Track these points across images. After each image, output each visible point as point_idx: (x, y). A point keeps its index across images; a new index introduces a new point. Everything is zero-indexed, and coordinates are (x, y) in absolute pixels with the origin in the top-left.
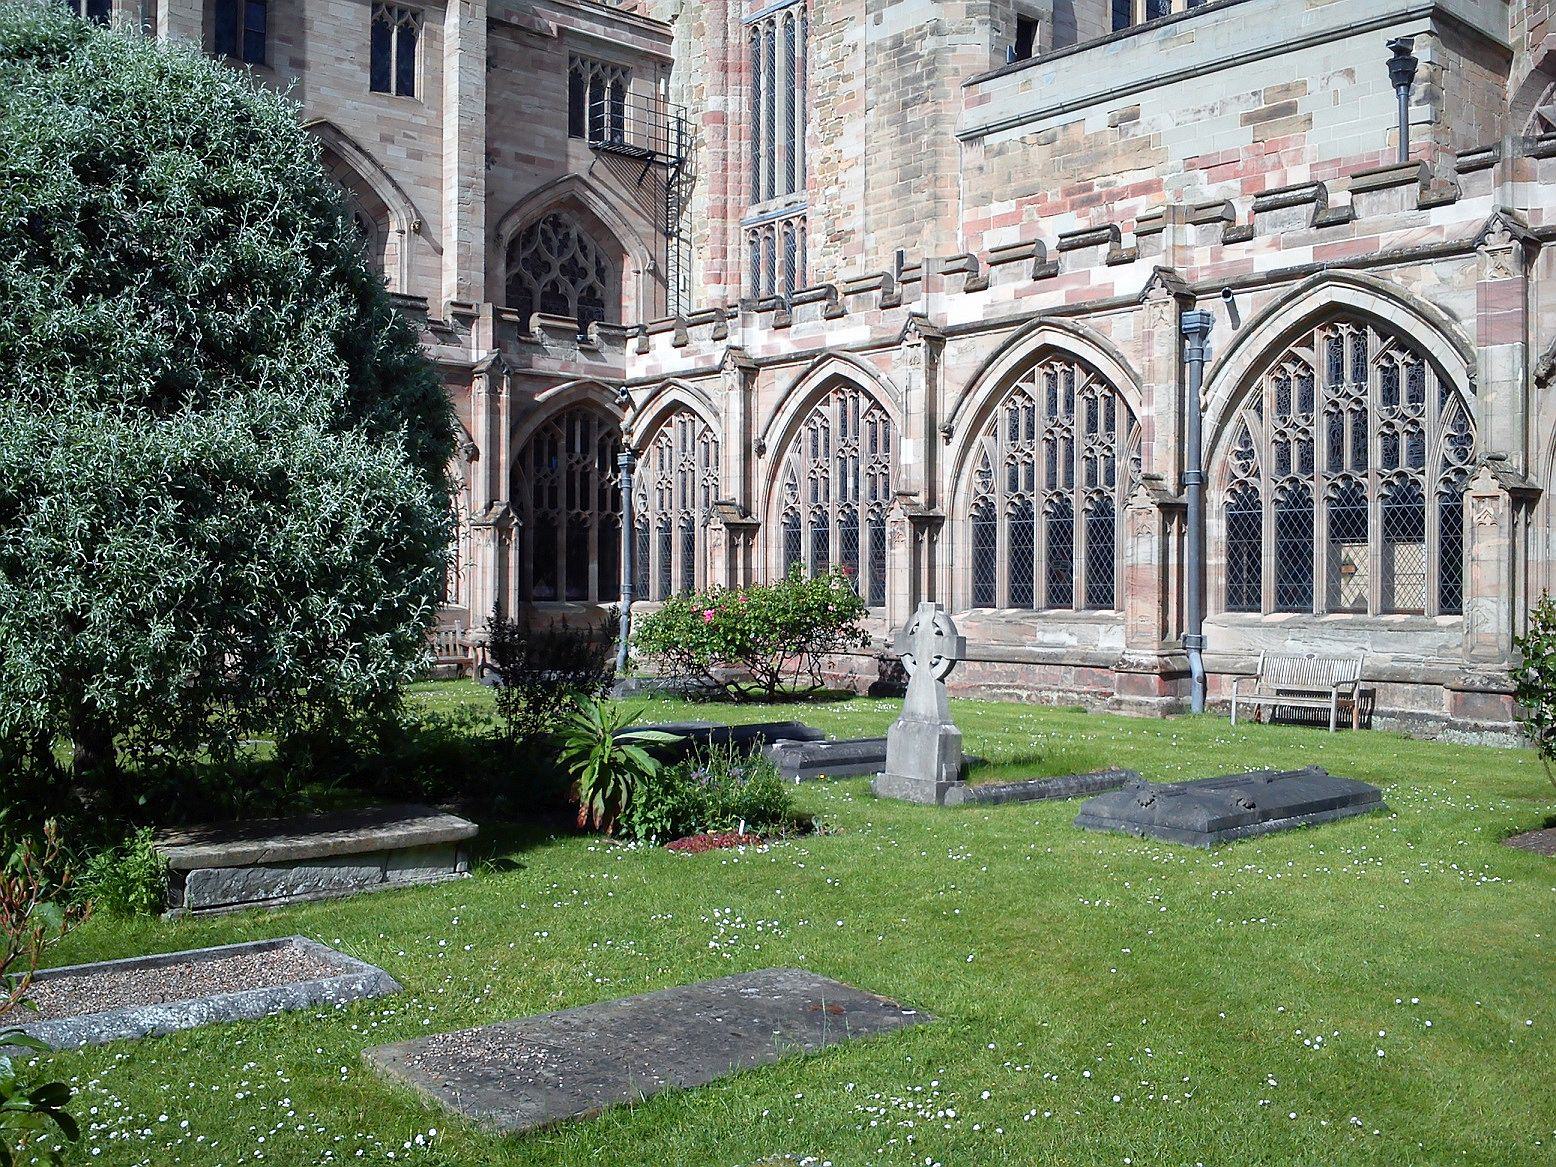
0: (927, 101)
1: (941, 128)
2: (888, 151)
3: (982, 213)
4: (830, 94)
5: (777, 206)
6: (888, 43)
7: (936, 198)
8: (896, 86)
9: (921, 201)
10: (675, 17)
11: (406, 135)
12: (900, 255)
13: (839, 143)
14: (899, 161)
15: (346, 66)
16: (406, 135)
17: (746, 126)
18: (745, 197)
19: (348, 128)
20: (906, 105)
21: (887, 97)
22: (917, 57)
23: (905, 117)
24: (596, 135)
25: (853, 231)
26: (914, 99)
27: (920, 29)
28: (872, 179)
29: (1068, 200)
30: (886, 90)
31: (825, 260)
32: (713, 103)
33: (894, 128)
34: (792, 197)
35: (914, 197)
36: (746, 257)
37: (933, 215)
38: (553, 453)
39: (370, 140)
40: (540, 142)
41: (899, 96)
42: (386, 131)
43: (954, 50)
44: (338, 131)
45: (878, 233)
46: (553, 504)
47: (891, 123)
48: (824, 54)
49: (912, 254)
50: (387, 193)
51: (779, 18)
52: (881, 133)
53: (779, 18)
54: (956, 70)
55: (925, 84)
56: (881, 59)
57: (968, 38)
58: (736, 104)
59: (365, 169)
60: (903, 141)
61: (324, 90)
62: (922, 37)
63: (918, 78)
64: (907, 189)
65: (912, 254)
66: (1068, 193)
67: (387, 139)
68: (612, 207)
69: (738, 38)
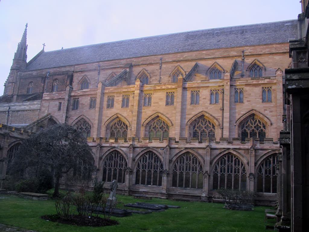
11: (269, 109)
16: (269, 109)
19: (258, 109)
38: (270, 164)
39: (262, 111)
42: (265, 109)
44: (255, 110)
46: (270, 174)
50: (266, 119)
67: (265, 110)
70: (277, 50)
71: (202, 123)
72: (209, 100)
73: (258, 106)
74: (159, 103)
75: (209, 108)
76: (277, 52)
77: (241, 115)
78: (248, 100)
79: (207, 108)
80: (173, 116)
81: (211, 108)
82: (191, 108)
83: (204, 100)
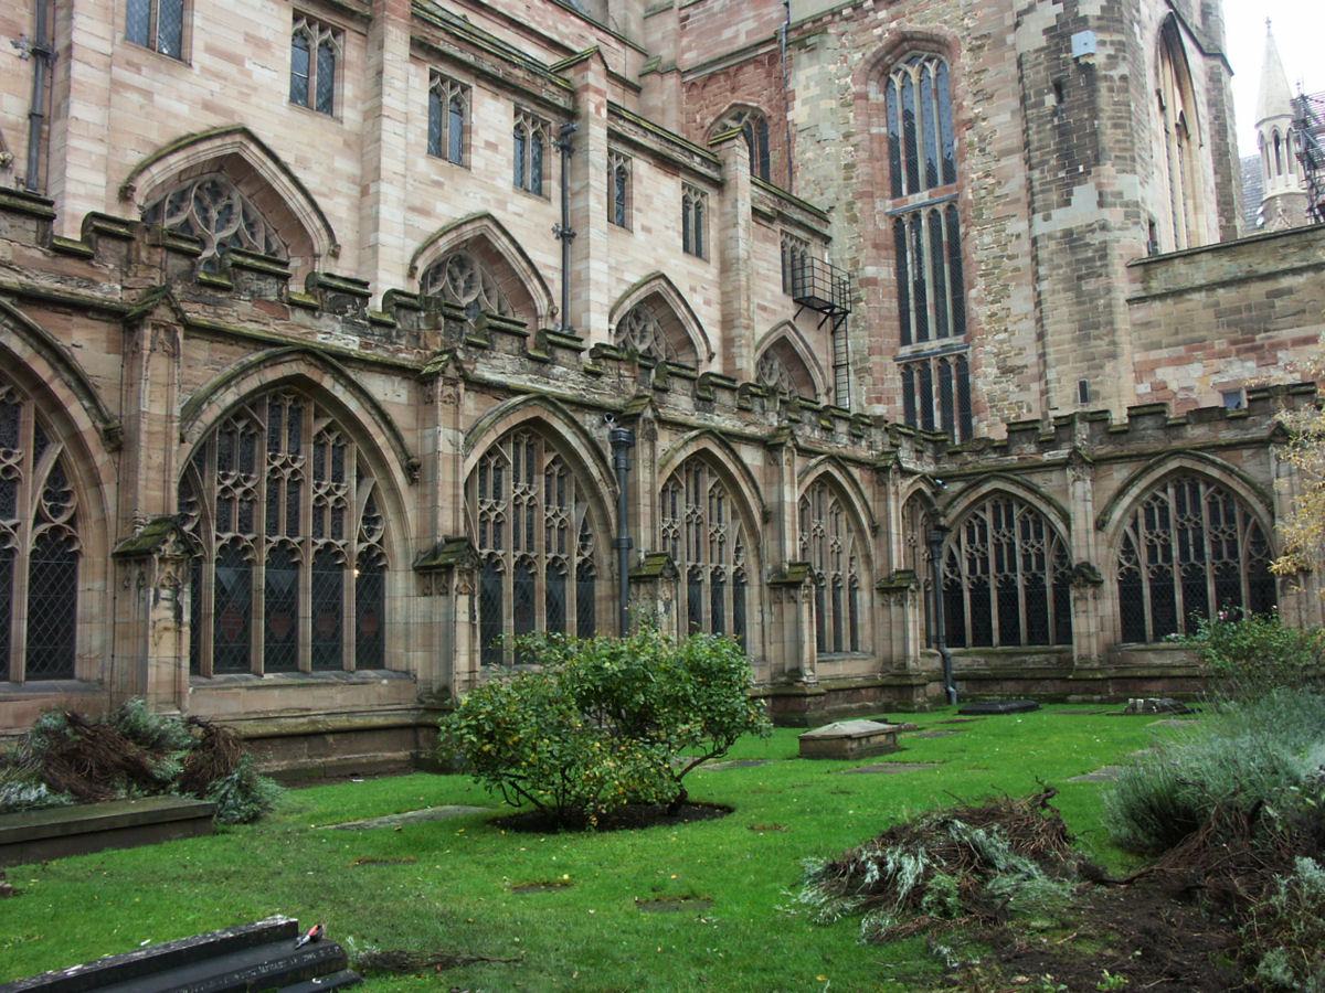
0: (1101, 275)
1: (1113, 295)
2: (1065, 309)
3: (1154, 355)
4: (995, 268)
5: (933, 344)
6: (1059, 234)
7: (1114, 343)
8: (1069, 264)
9: (1102, 345)
10: (832, 208)
12: (1083, 386)
13: (1006, 303)
14: (1077, 317)
15: (671, 233)
17: (894, 289)
18: (896, 340)
20: (1080, 278)
21: (1061, 272)
22: (1088, 245)
23: (1079, 287)
24: (794, 289)
25: (1026, 366)
26: (1088, 274)
27: (1091, 225)
28: (1050, 328)
29: (1233, 348)
30: (1059, 267)
31: (997, 387)
32: (870, 271)
33: (1070, 294)
34: (946, 341)
35: (1093, 343)
36: (899, 384)
37: (1113, 356)
40: (769, 295)
41: (1074, 270)
42: (693, 283)
43: (1118, 241)
44: (669, 283)
45: (1059, 368)
47: (1066, 290)
48: (987, 239)
49: (1096, 383)
50: (693, 331)
51: (924, 213)
52: (1056, 296)
53: (924, 213)
54: (1121, 256)
55: (1098, 264)
56: (1052, 245)
57: (1126, 233)
58: (884, 272)
59: (681, 312)
60: (1079, 303)
61: (660, 251)
62: (1093, 231)
63: (1092, 259)
64: (1088, 337)
65: (1096, 383)
66: (1234, 342)
67: (693, 289)
68: (807, 346)
69: (885, 226)
70: (533, 18)
71: (453, 280)
72: (508, 160)
73: (673, 261)
74: (248, 65)
75: (510, 207)
76: (533, 26)
77: (625, 287)
78: (646, 223)
79: (502, 204)
80: (338, 192)
81: (520, 211)
82: (436, 178)
83: (488, 153)
